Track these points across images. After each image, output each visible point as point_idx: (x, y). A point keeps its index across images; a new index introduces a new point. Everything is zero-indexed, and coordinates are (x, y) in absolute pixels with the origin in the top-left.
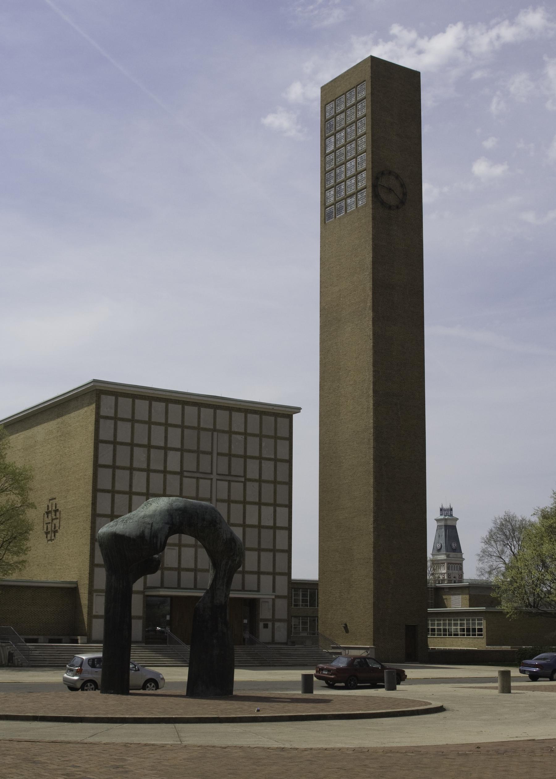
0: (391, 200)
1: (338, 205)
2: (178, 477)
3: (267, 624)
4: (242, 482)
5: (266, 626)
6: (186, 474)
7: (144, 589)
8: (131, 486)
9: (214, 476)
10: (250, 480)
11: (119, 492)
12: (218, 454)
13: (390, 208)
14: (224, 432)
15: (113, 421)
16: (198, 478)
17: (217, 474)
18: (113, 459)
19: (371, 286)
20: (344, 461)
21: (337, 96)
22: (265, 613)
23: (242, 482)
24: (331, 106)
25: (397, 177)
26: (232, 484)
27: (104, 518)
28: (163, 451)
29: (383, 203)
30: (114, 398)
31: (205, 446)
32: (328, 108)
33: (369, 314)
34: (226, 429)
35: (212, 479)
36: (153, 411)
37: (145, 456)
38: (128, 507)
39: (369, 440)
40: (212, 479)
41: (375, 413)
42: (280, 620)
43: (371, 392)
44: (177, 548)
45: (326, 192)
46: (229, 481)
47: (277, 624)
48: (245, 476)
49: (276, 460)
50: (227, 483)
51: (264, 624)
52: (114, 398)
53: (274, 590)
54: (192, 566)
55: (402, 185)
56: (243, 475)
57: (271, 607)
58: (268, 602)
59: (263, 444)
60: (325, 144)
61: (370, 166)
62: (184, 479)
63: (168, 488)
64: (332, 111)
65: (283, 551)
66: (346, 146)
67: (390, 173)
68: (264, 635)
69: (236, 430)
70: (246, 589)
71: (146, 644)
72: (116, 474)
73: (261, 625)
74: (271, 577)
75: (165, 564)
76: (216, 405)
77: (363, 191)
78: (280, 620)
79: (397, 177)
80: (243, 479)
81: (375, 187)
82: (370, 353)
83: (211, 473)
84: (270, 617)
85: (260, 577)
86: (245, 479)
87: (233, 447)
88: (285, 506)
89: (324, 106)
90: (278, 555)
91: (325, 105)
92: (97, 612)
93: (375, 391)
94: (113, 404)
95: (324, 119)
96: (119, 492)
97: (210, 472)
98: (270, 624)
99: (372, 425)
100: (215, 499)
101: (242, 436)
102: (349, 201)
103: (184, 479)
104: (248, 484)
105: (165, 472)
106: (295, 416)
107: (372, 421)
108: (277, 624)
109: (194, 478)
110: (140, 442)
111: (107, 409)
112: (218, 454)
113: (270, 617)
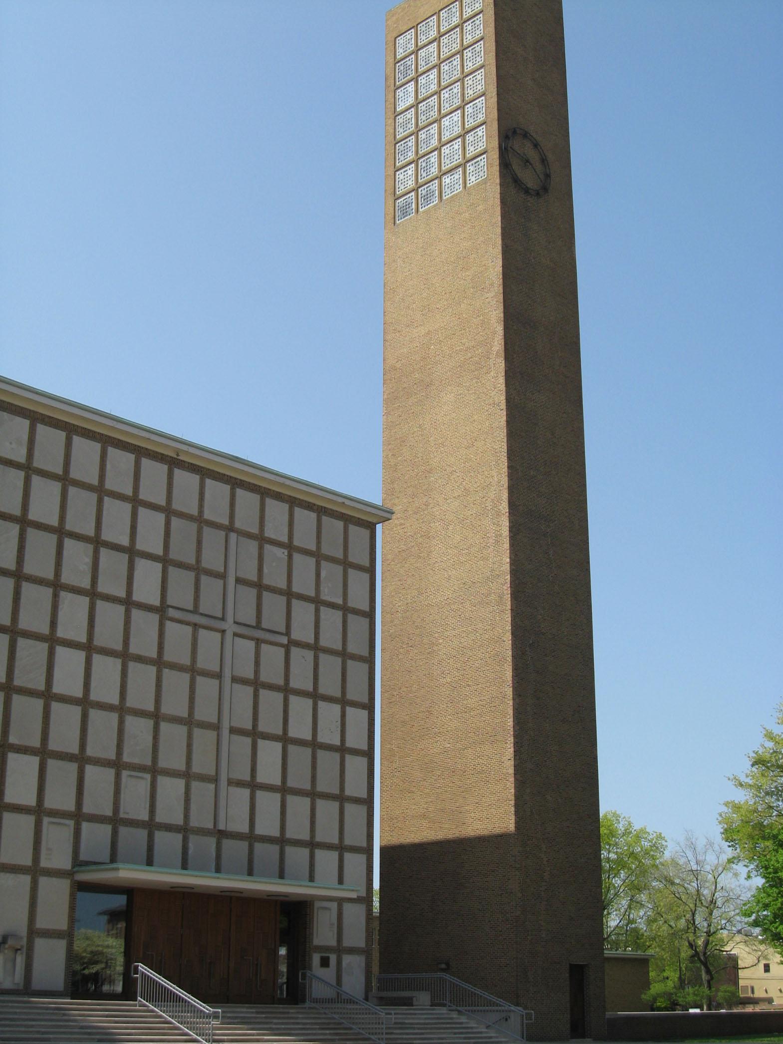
0: (530, 179)
1: (422, 191)
2: (156, 617)
3: (328, 958)
4: (282, 645)
5: (325, 962)
6: (171, 613)
7: (73, 867)
8: (53, 624)
9: (229, 626)
10: (298, 644)
11: (27, 635)
12: (238, 581)
13: (527, 191)
14: (249, 535)
15: (22, 474)
16: (196, 626)
17: (235, 622)
18: (18, 557)
19: (502, 315)
20: (441, 641)
21: (419, 21)
23: (282, 645)
24: (409, 37)
25: (536, 145)
26: (264, 647)
28: (125, 557)
29: (516, 181)
30: (27, 423)
31: (212, 559)
32: (401, 41)
33: (499, 366)
34: (252, 531)
35: (223, 632)
36: (108, 466)
37: (88, 560)
38: (45, 670)
40: (223, 632)
41: (512, 545)
42: (351, 951)
43: (504, 507)
44: (148, 776)
45: (397, 173)
46: (258, 642)
47: (347, 959)
48: (288, 633)
49: (345, 610)
52: (27, 423)
53: (341, 881)
54: (179, 820)
55: (544, 161)
57: (335, 921)
59: (323, 574)
60: (395, 98)
61: (495, 114)
62: (169, 625)
63: (132, 640)
64: (409, 46)
65: (357, 801)
66: (440, 93)
67: (526, 135)
69: (273, 536)
73: (316, 959)
74: (335, 855)
76: (236, 479)
77: (479, 159)
78: (351, 951)
79: (536, 145)
80: (284, 640)
81: (504, 152)
82: (501, 434)
83: (223, 619)
85: (314, 852)
87: (265, 570)
88: (363, 706)
89: (393, 39)
90: (349, 808)
91: (396, 38)
93: (511, 504)
94: (25, 437)
95: (393, 59)
96: (27, 635)
97: (220, 615)
98: (333, 958)
99: (507, 567)
100: (231, 676)
101: (283, 550)
102: (447, 180)
103: (169, 625)
104: (294, 650)
105: (128, 603)
107: (508, 560)
108: (347, 959)
109: (188, 623)
111: (11, 443)
112: (238, 581)
113: (333, 943)
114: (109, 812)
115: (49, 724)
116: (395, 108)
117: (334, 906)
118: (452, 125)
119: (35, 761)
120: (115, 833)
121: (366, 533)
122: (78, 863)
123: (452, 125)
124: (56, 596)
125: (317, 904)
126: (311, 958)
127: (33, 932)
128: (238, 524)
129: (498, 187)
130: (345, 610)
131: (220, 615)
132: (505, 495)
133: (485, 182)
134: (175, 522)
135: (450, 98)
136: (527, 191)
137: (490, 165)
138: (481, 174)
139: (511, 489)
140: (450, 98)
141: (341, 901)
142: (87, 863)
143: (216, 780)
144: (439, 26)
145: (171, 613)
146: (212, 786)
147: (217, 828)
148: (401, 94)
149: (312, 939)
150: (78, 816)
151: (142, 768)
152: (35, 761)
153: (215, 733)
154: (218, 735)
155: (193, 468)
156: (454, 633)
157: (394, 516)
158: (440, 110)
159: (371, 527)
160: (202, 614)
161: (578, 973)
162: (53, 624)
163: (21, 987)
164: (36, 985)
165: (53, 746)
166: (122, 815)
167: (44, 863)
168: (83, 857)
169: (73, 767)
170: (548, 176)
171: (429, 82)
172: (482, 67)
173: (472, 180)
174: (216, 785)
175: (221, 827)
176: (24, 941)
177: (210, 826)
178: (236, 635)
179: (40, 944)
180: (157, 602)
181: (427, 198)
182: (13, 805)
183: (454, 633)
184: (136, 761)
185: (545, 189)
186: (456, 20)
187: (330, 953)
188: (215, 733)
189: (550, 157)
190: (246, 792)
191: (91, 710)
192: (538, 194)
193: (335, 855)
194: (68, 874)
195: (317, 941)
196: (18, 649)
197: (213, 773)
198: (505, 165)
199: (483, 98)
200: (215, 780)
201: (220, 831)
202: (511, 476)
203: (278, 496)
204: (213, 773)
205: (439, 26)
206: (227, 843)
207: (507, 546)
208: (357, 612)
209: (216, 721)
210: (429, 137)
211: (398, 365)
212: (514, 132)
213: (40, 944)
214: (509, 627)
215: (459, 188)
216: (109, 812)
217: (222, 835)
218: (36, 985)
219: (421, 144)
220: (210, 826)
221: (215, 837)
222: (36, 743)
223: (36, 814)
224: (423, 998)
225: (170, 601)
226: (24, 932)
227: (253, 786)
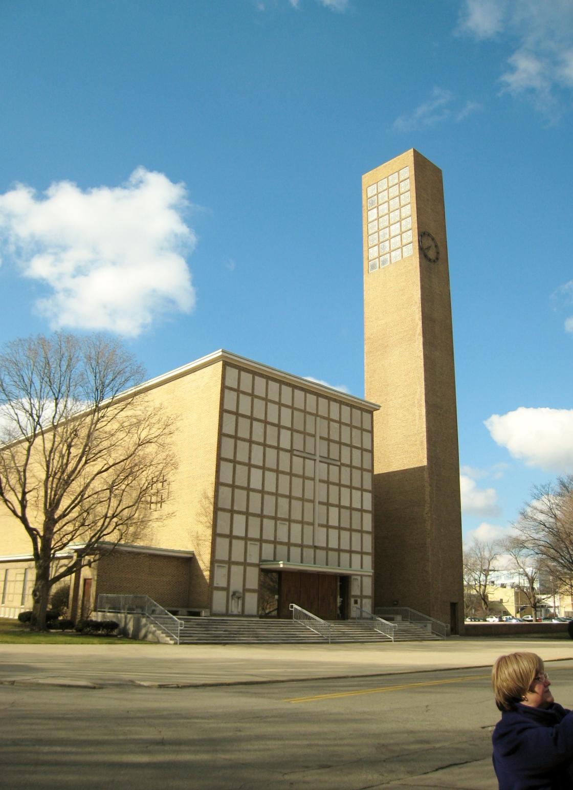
4: (337, 466)
5: (356, 602)
7: (260, 561)
8: (250, 458)
11: (240, 463)
13: (430, 260)
16: (304, 458)
22: (355, 590)
23: (337, 466)
25: (433, 239)
35: (315, 460)
36: (269, 390)
39: (422, 442)
40: (315, 460)
41: (427, 420)
42: (366, 597)
47: (365, 601)
48: (340, 460)
49: (362, 449)
50: (326, 465)
54: (299, 542)
55: (436, 246)
56: (338, 459)
58: (357, 579)
59: (353, 434)
67: (429, 235)
68: (354, 611)
72: (238, 444)
73: (352, 600)
74: (359, 556)
78: (366, 597)
79: (433, 239)
82: (422, 370)
83: (315, 455)
86: (341, 464)
92: (217, 584)
93: (426, 402)
96: (240, 463)
102: (393, 254)
106: (375, 413)
109: (301, 457)
110: (258, 417)
113: (359, 594)
114: (272, 539)
116: (368, 220)
117: (359, 578)
118: (395, 229)
120: (275, 548)
121: (370, 415)
122: (261, 560)
123: (395, 229)
124: (250, 446)
125: (353, 577)
126: (350, 599)
127: (245, 590)
128: (319, 413)
129: (418, 259)
130: (362, 449)
131: (313, 453)
132: (423, 397)
133: (411, 256)
134: (296, 413)
135: (395, 216)
136: (430, 260)
137: (414, 249)
138: (410, 252)
139: (427, 395)
140: (395, 216)
141: (362, 576)
144: (388, 184)
145: (295, 452)
146: (312, 527)
148: (381, 221)
150: (261, 541)
151: (285, 520)
153: (312, 504)
154: (314, 505)
155: (302, 389)
156: (400, 457)
157: (381, 408)
158: (389, 222)
159: (371, 413)
160: (307, 453)
161: (454, 605)
162: (250, 458)
163: (241, 614)
164: (246, 613)
166: (278, 540)
167: (248, 561)
168: (263, 558)
170: (438, 253)
171: (384, 208)
172: (409, 203)
173: (405, 255)
175: (316, 544)
176: (242, 595)
178: (320, 461)
179: (248, 595)
180: (289, 448)
181: (384, 262)
183: (400, 457)
184: (283, 516)
185: (437, 259)
186: (396, 181)
189: (439, 244)
190: (325, 529)
192: (434, 261)
193: (359, 556)
194: (258, 565)
195: (353, 593)
196: (237, 470)
198: (421, 249)
199: (410, 218)
200: (313, 524)
202: (426, 389)
203: (335, 400)
205: (388, 184)
206: (318, 551)
207: (424, 420)
208: (366, 450)
209: (313, 499)
210: (385, 234)
211: (372, 337)
212: (424, 233)
213: (248, 595)
214: (426, 456)
215: (399, 258)
216: (272, 539)
217: (316, 548)
218: (246, 613)
219: (381, 237)
220: (311, 544)
224: (399, 618)
225: (294, 448)
226: (241, 590)
227: (328, 527)
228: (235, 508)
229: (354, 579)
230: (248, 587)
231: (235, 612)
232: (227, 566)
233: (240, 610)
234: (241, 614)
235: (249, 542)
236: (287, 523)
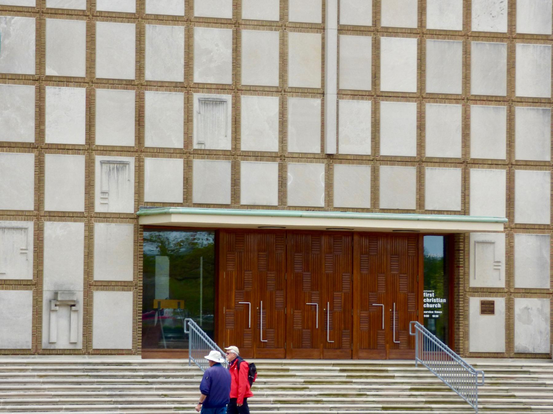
3: (492, 303)
7: (137, 208)
27: (16, 18)
42: (528, 293)
47: (520, 303)
51: (483, 303)
57: (503, 259)
70: (428, 206)
71: (143, 358)
73: (474, 303)
75: (195, 141)
78: (528, 293)
84: (501, 284)
85: (469, 173)
98: (500, 303)
108: (520, 303)
113: (501, 284)
115: (94, 49)
119: (80, 93)
125: (474, 238)
126: (466, 302)
142: (154, 205)
143: (323, 94)
146: (317, 102)
147: (325, 153)
149: (468, 280)
152: (80, 93)
154: (323, 38)
163: (80, 346)
164: (96, 344)
165: (101, 73)
167: (99, 208)
168: (148, 197)
169: (130, 96)
174: (323, 100)
175: (331, 150)
176: (80, 296)
177: (317, 149)
179: (99, 296)
182: (57, 145)
184: (211, 80)
187: (496, 296)
188: (319, 36)
191: (147, 26)
195: (474, 283)
197: (318, 85)
201: (330, 156)
204: (318, 85)
206: (339, 169)
209: (319, 21)
213: (99, 296)
218: (96, 344)
220: (317, 149)
221: (323, 163)
222: (80, 71)
223: (86, 153)
228: (50, 71)
229: (477, 242)
230: (99, 275)
231: (63, 344)
232: (30, 225)
233: (77, 336)
234: (80, 346)
235: (98, 159)
236: (228, 98)
